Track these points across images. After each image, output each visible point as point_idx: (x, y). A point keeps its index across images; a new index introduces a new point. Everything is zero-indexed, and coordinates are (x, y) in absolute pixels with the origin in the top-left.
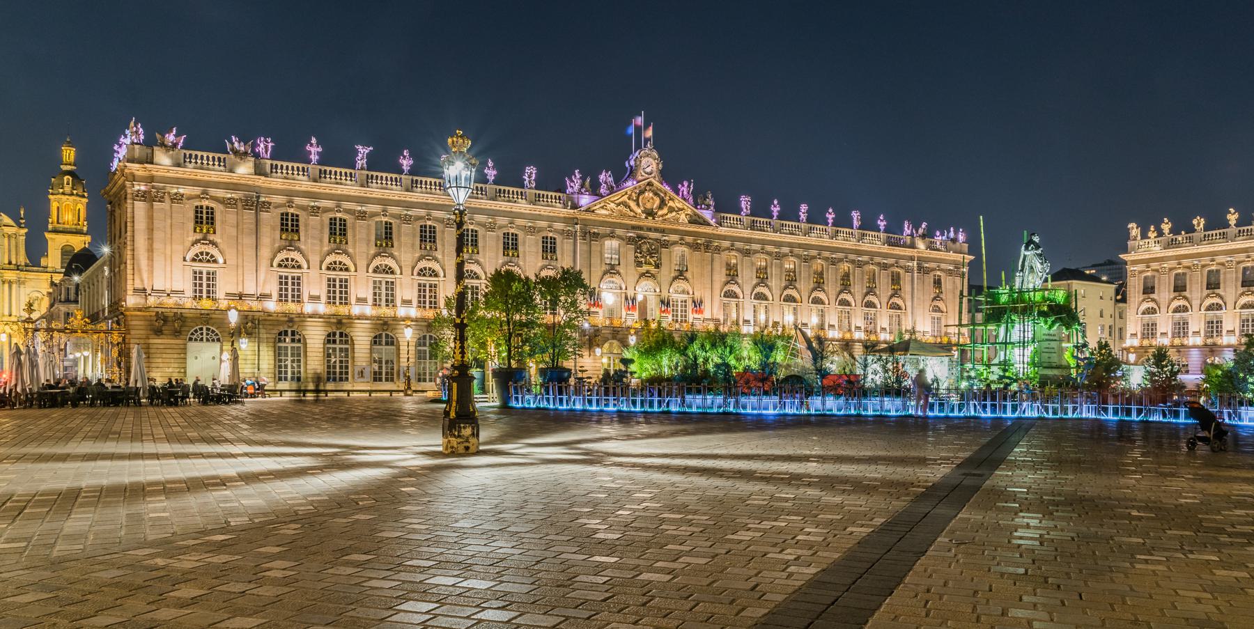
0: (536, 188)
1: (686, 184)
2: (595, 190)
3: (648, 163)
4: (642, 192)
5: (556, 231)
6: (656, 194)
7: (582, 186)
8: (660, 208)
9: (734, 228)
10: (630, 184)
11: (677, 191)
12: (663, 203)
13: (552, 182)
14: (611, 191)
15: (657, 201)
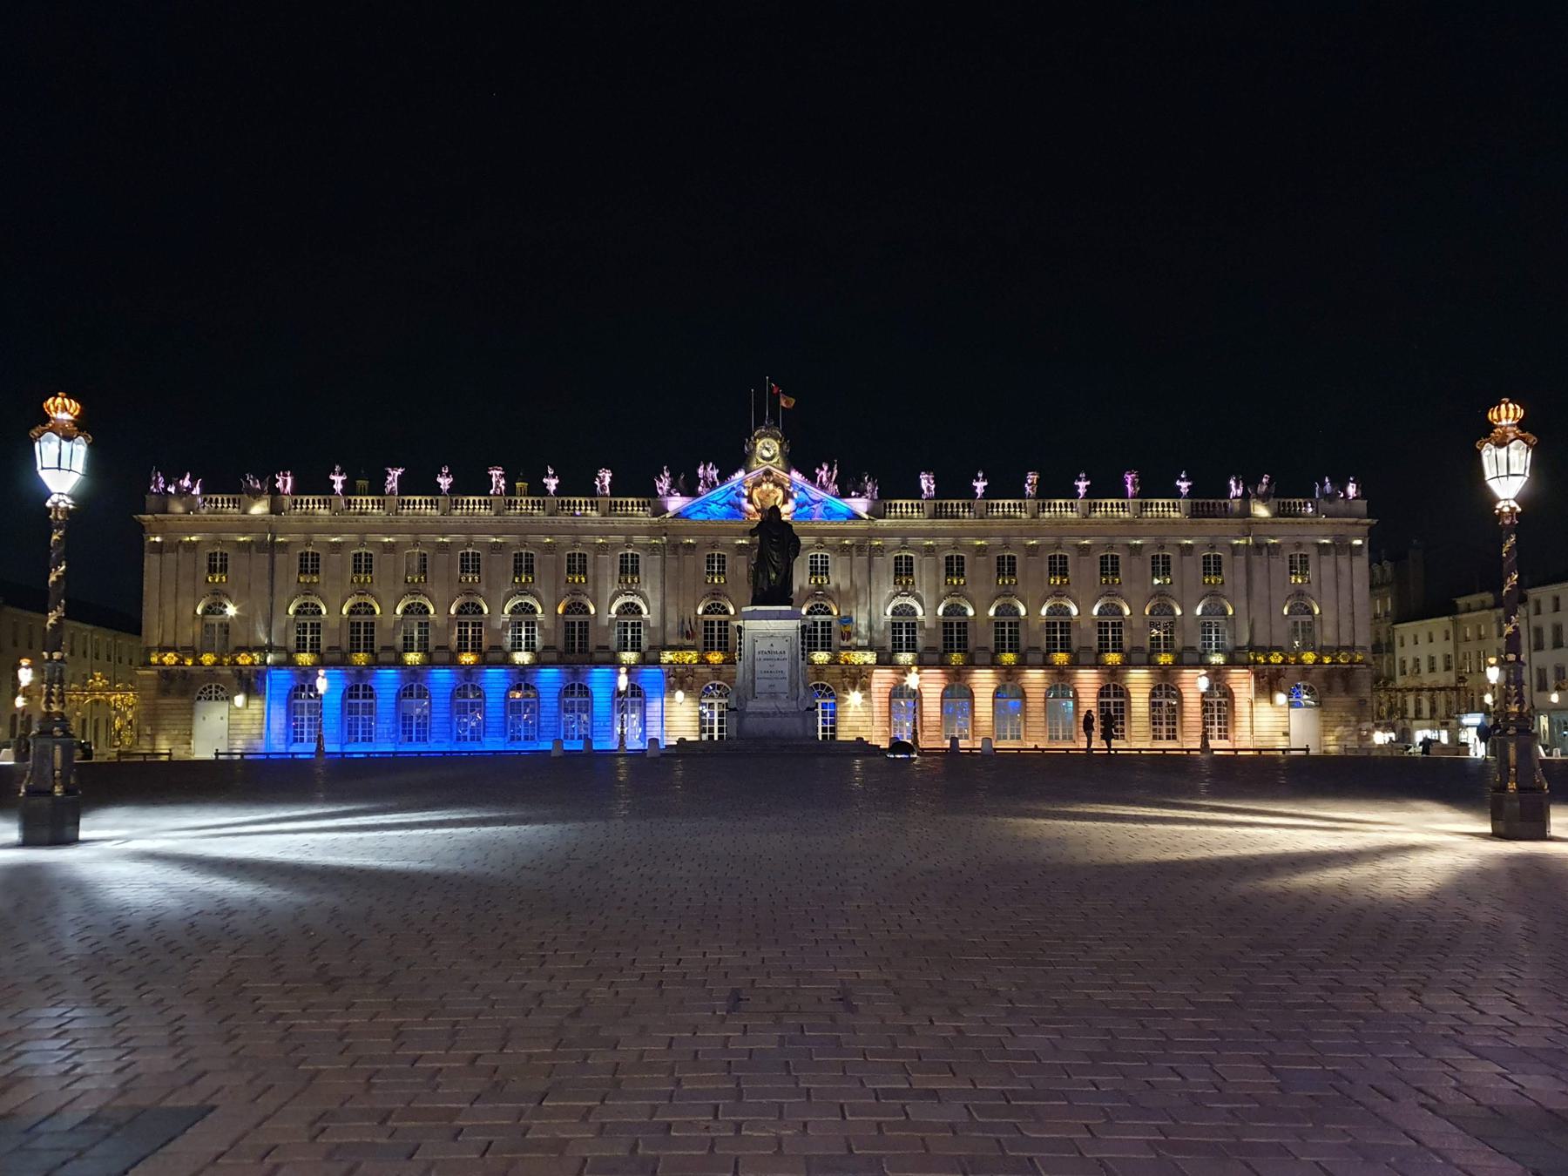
0: (612, 495)
1: (826, 468)
2: (690, 490)
3: (767, 448)
4: (757, 484)
5: (637, 546)
6: (778, 484)
7: (672, 486)
8: (785, 502)
9: (908, 515)
10: (740, 475)
11: (812, 478)
12: (788, 496)
13: (636, 484)
14: (713, 486)
15: (780, 493)
